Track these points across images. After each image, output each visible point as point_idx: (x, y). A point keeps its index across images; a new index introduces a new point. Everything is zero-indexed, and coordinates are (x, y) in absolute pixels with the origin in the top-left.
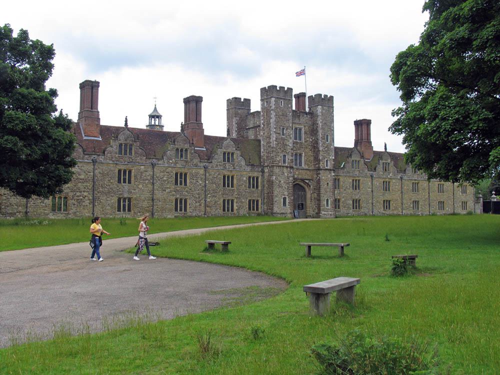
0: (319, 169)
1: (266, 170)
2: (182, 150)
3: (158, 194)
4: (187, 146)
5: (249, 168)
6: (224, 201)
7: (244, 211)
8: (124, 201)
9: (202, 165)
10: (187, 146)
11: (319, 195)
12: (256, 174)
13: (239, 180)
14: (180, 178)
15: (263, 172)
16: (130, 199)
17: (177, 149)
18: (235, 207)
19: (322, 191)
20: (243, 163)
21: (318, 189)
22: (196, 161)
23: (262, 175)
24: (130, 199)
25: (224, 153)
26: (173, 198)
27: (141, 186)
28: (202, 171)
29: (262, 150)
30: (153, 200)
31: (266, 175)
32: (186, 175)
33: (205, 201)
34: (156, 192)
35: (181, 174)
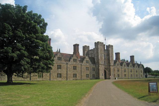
0: (110, 65)
1: (97, 66)
2: (75, 59)
3: (68, 72)
4: (76, 58)
5: (92, 65)
6: (86, 74)
7: (92, 77)
8: (59, 74)
9: (80, 64)
10: (76, 58)
11: (110, 73)
12: (94, 67)
13: (90, 68)
14: (75, 68)
15: (96, 66)
16: (61, 74)
17: (74, 59)
18: (89, 76)
19: (111, 72)
20: (91, 63)
21: (110, 71)
22: (79, 62)
23: (96, 67)
24: (61, 74)
25: (86, 60)
26: (73, 74)
27: (64, 70)
28: (80, 66)
29: (95, 60)
30: (67, 74)
31: (97, 67)
32: (76, 67)
33: (81, 74)
34: (68, 72)
35: (75, 67)
